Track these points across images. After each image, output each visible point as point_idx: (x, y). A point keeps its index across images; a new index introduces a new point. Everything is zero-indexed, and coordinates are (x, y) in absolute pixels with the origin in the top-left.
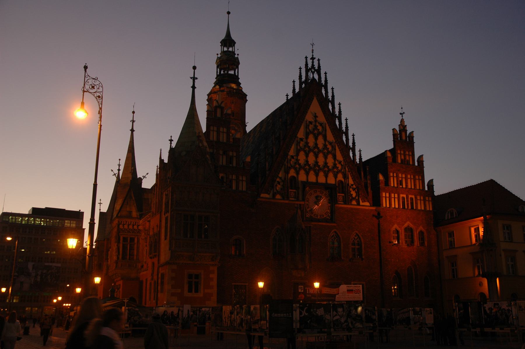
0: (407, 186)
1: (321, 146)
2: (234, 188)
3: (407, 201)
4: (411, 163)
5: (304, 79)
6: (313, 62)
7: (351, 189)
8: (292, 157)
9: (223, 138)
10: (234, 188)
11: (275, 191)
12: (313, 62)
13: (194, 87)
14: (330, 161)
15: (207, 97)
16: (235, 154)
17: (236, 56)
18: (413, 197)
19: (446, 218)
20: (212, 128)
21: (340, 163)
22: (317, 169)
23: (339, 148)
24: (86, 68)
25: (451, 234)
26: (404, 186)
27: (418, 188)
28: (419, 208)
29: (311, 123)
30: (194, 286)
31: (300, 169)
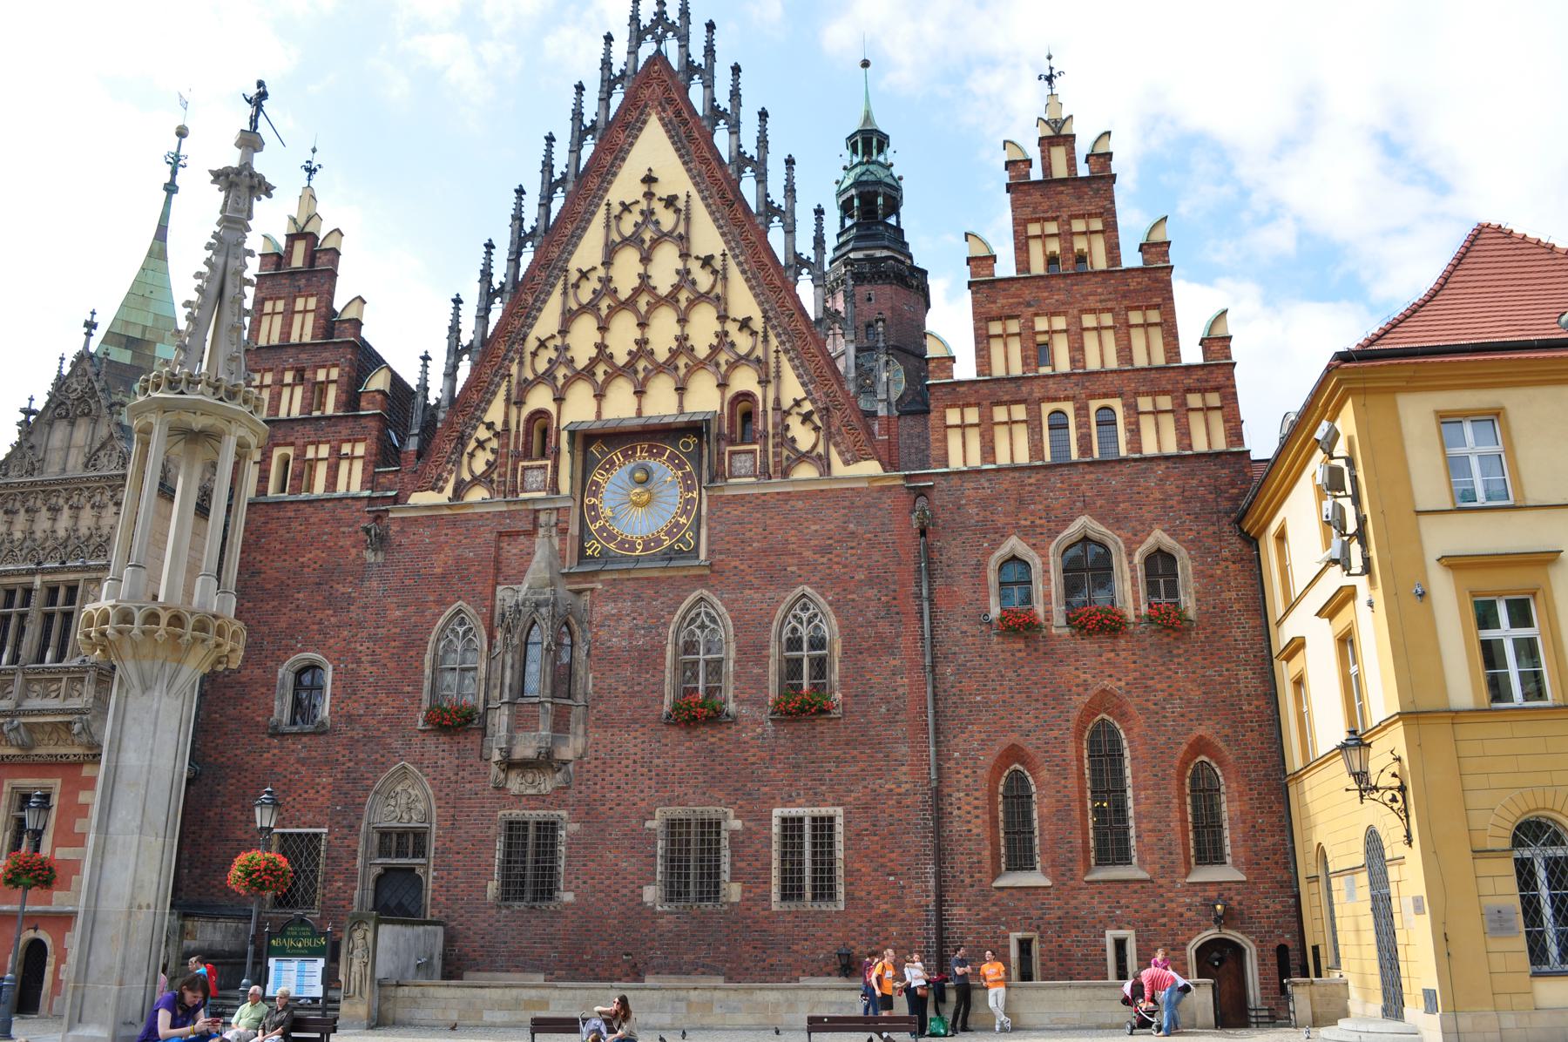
0: (1073, 361)
2: (319, 488)
3: (1083, 425)
4: (1100, 262)
7: (794, 422)
8: (542, 344)
10: (319, 488)
11: (467, 477)
13: (171, 188)
16: (334, 374)
18: (1116, 404)
20: (268, 307)
21: (745, 324)
22: (639, 368)
23: (743, 272)
25: (1281, 537)
26: (1063, 363)
27: (1140, 361)
28: (1149, 449)
29: (626, 208)
31: (569, 382)
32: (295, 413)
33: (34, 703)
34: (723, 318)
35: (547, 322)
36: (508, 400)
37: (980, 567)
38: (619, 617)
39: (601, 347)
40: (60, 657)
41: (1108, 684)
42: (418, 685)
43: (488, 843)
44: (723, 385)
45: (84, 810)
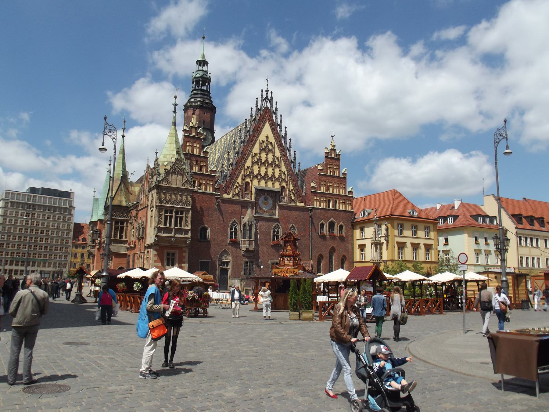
1: (270, 160)
5: (259, 107)
6: (267, 94)
8: (248, 167)
9: (196, 152)
12: (267, 94)
13: (175, 112)
14: (277, 171)
15: (183, 108)
17: (208, 75)
19: (360, 216)
22: (266, 178)
24: (105, 118)
29: (263, 142)
30: (171, 262)
32: (197, 171)
33: (177, 235)
34: (280, 171)
35: (249, 163)
36: (242, 178)
37: (318, 224)
38: (263, 226)
39: (259, 171)
40: (181, 226)
41: (333, 245)
42: (227, 234)
43: (241, 265)
44: (280, 184)
45: (184, 257)
